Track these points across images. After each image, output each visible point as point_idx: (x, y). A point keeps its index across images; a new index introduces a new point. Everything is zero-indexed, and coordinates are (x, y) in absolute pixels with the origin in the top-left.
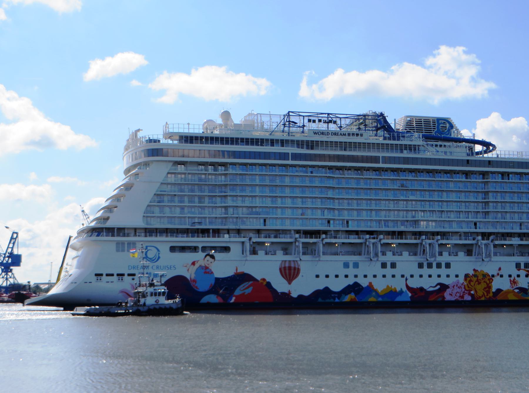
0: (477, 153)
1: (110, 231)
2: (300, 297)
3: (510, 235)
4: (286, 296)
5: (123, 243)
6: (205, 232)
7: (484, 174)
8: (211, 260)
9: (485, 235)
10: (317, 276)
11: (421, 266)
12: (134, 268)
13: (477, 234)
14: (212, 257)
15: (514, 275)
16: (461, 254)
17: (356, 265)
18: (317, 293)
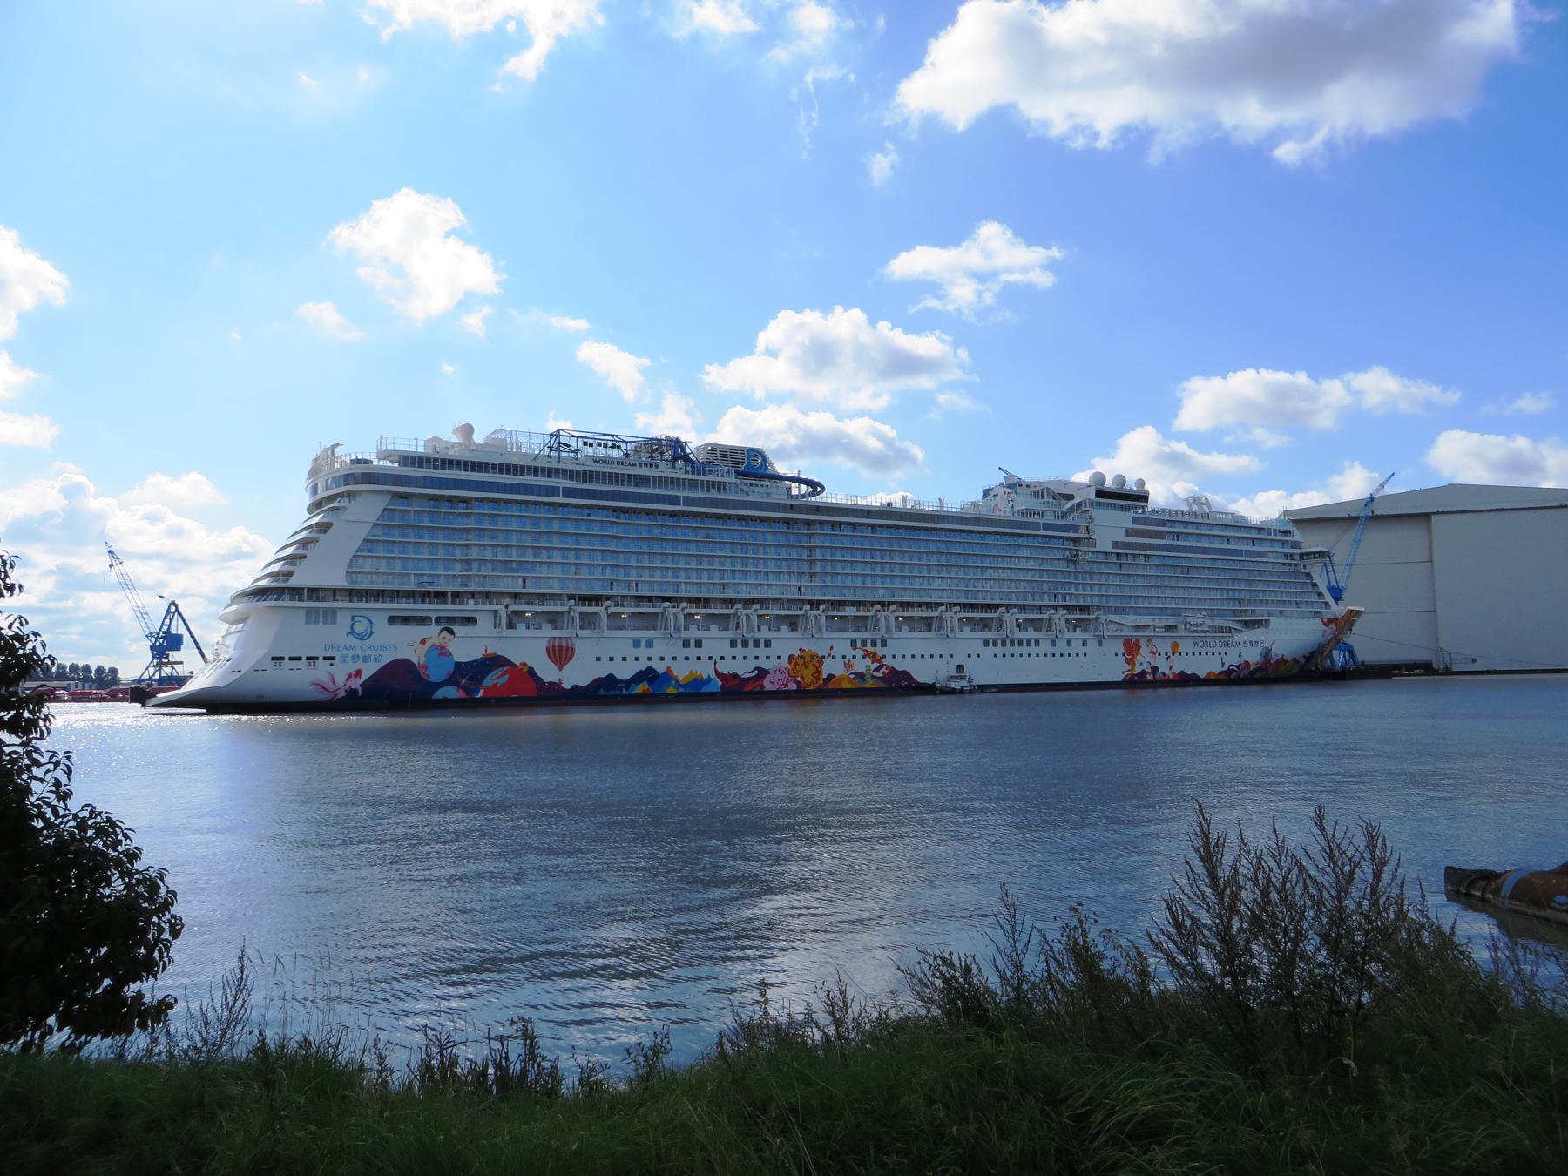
0: (803, 496)
1: (296, 592)
2: (575, 688)
3: (842, 604)
4: (555, 686)
5: (317, 610)
6: (440, 596)
7: (808, 523)
8: (450, 636)
9: (814, 604)
10: (598, 659)
11: (733, 644)
12: (333, 647)
13: (803, 602)
14: (451, 632)
15: (849, 656)
16: (784, 628)
17: (650, 644)
18: (598, 683)
